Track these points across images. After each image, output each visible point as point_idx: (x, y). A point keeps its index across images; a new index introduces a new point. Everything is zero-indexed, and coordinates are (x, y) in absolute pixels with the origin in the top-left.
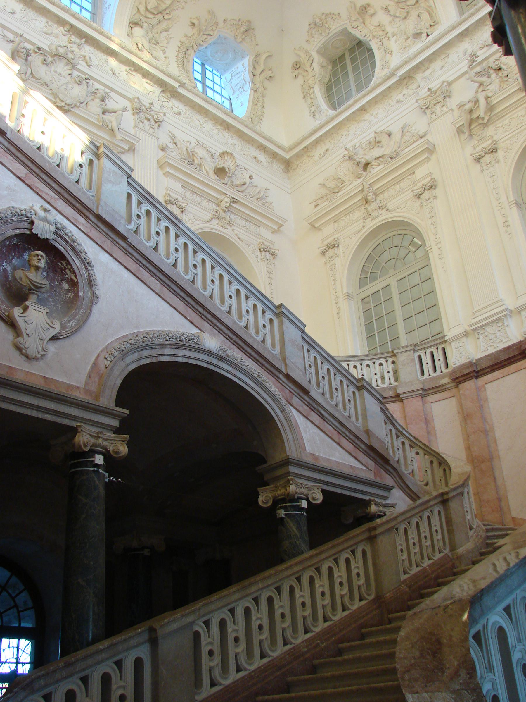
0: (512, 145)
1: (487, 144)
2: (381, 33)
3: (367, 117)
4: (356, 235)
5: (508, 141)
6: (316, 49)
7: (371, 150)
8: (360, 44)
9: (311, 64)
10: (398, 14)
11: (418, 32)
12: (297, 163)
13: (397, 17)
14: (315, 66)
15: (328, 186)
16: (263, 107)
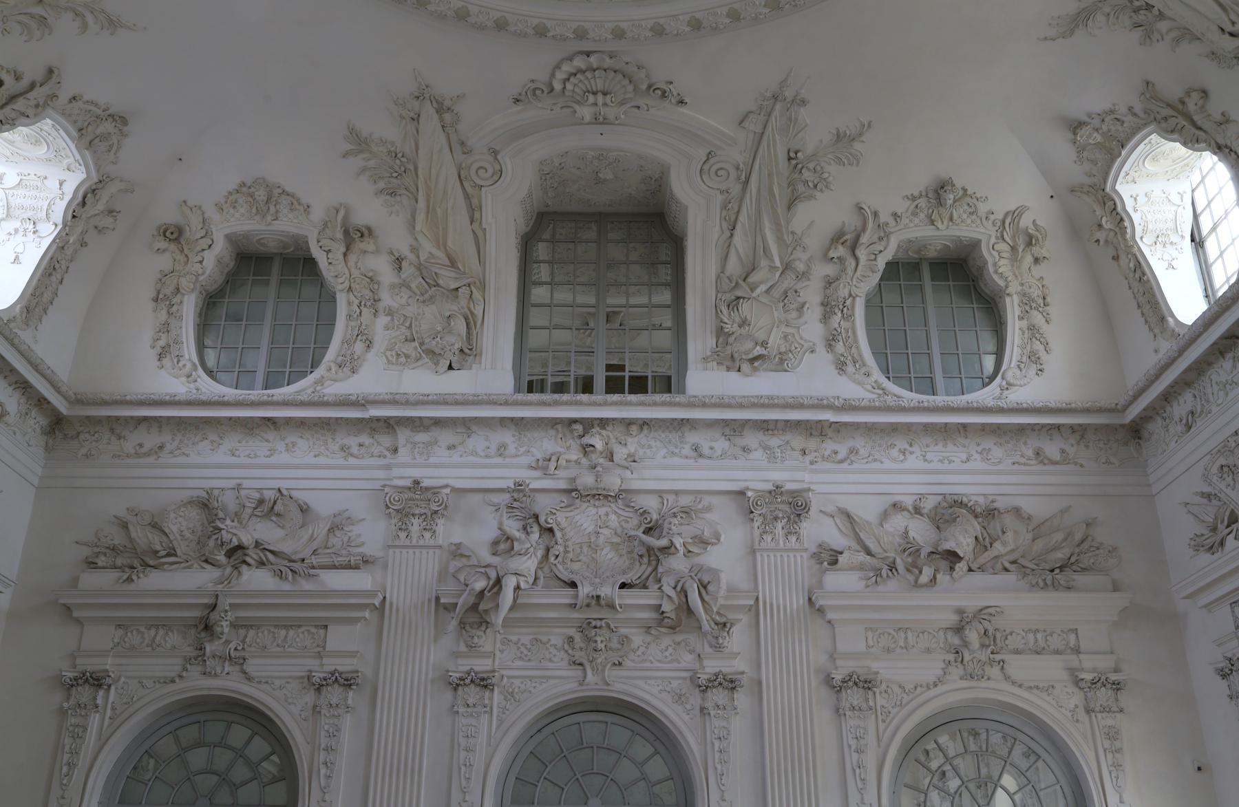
0: (522, 693)
1: (481, 665)
2: (367, 292)
3: (271, 435)
4: (158, 686)
5: (517, 682)
6: (228, 231)
7: (254, 518)
8: (309, 263)
9: (203, 250)
10: (413, 286)
11: (437, 351)
12: (82, 428)
13: (409, 288)
14: (210, 258)
15: (133, 535)
16: (61, 282)
